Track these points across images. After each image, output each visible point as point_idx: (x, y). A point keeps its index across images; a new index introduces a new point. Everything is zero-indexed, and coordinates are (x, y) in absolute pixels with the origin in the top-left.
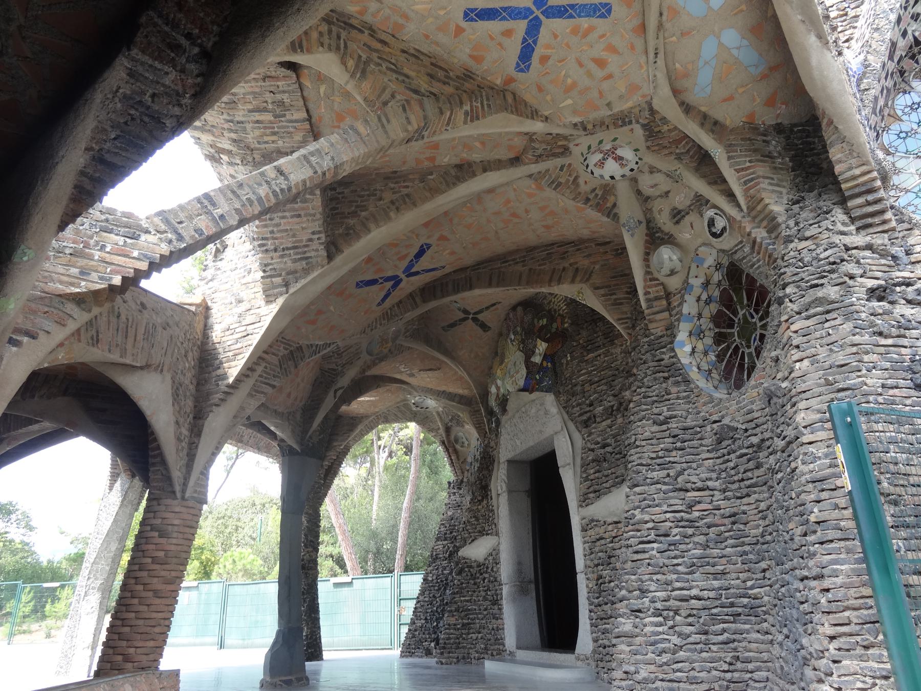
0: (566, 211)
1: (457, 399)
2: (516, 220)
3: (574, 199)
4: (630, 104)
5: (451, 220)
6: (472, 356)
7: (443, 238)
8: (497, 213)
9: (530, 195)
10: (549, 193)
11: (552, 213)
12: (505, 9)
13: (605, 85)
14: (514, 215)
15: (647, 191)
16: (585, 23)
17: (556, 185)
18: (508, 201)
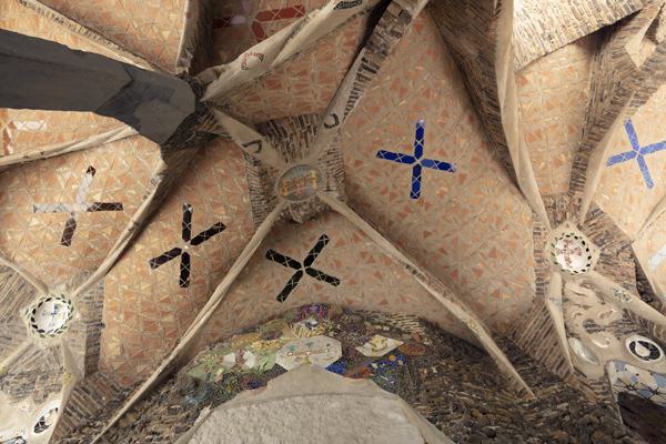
0: (523, 253)
1: (91, 350)
2: (493, 225)
3: (535, 251)
4: (625, 231)
5: (482, 176)
6: (239, 306)
7: (463, 177)
8: (496, 206)
9: (521, 221)
10: (530, 232)
11: (514, 246)
12: (635, 136)
13: (625, 210)
14: (499, 220)
15: (570, 295)
16: (642, 179)
17: (537, 233)
18: (510, 209)
